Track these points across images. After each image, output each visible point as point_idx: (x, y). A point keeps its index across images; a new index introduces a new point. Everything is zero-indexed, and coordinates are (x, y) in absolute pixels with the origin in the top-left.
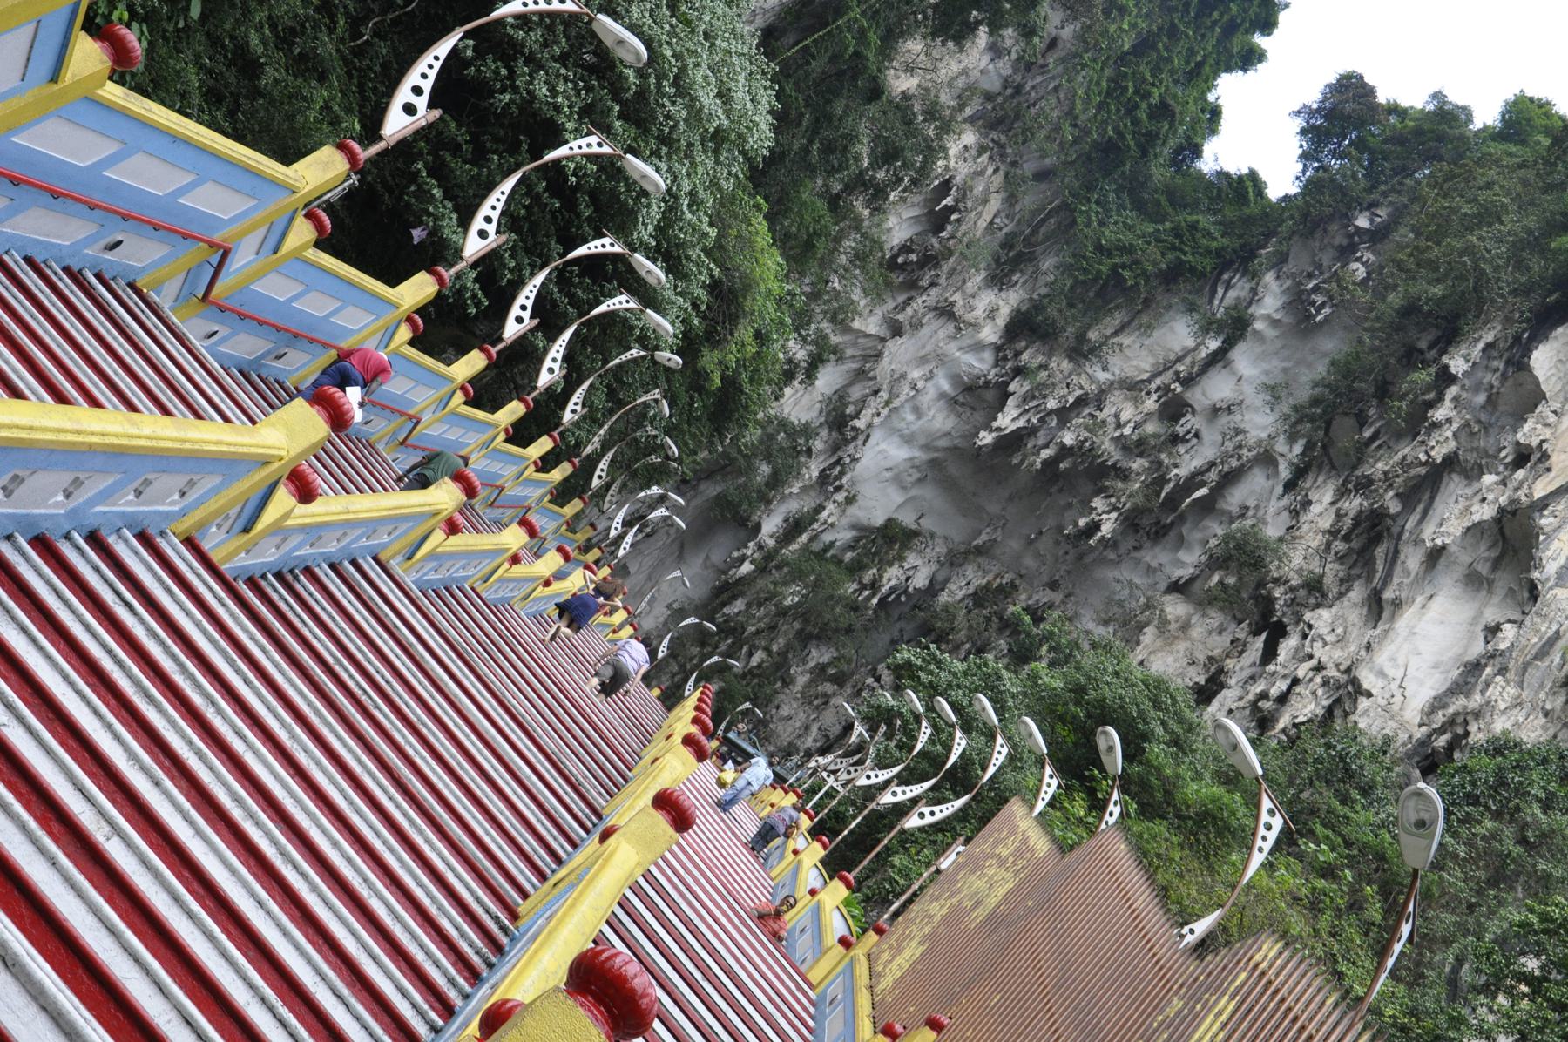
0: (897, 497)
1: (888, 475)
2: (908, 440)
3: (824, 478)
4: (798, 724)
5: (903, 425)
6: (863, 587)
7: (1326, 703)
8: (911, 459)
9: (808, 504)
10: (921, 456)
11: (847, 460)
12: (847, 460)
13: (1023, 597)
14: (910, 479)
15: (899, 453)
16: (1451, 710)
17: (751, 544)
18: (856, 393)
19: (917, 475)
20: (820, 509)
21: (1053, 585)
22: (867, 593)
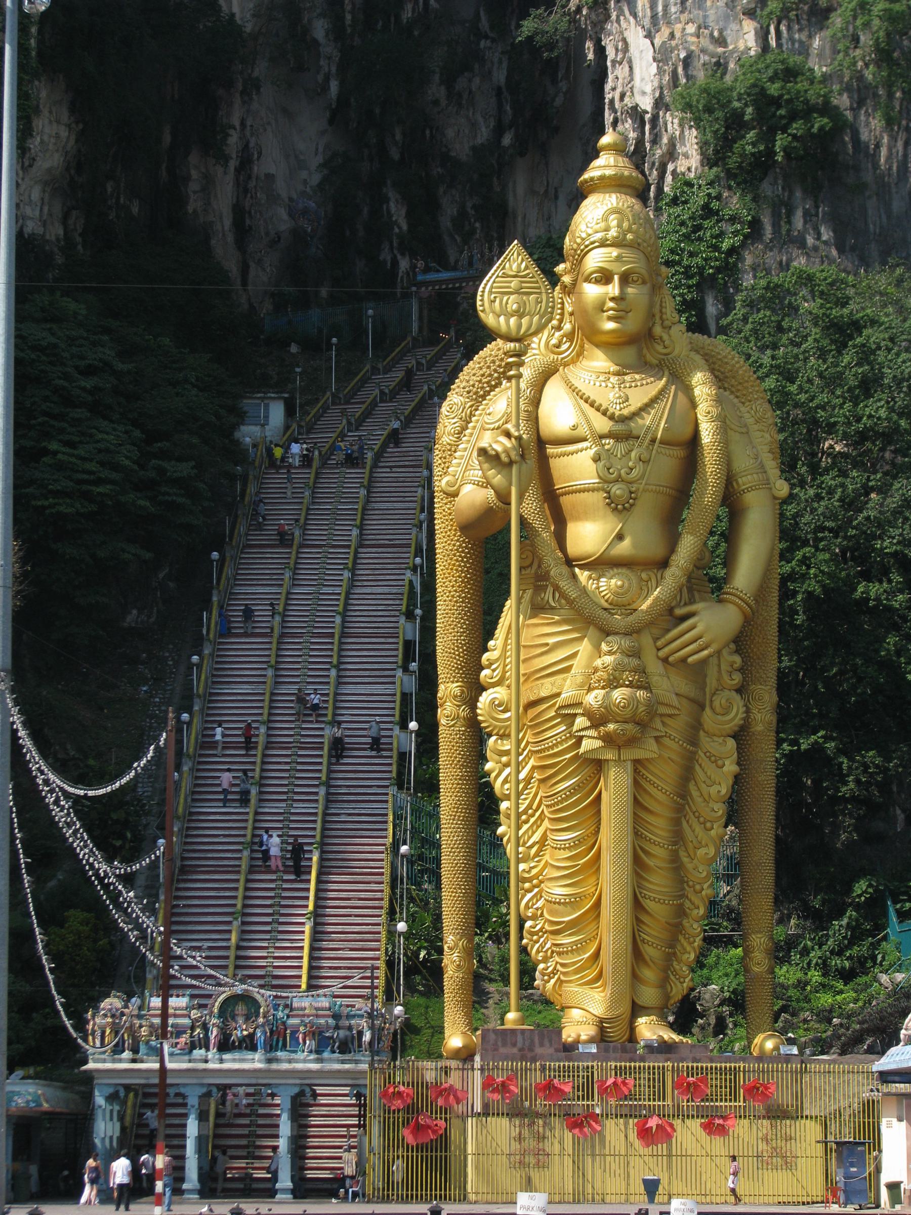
4: (467, 131)
17: (322, 63)
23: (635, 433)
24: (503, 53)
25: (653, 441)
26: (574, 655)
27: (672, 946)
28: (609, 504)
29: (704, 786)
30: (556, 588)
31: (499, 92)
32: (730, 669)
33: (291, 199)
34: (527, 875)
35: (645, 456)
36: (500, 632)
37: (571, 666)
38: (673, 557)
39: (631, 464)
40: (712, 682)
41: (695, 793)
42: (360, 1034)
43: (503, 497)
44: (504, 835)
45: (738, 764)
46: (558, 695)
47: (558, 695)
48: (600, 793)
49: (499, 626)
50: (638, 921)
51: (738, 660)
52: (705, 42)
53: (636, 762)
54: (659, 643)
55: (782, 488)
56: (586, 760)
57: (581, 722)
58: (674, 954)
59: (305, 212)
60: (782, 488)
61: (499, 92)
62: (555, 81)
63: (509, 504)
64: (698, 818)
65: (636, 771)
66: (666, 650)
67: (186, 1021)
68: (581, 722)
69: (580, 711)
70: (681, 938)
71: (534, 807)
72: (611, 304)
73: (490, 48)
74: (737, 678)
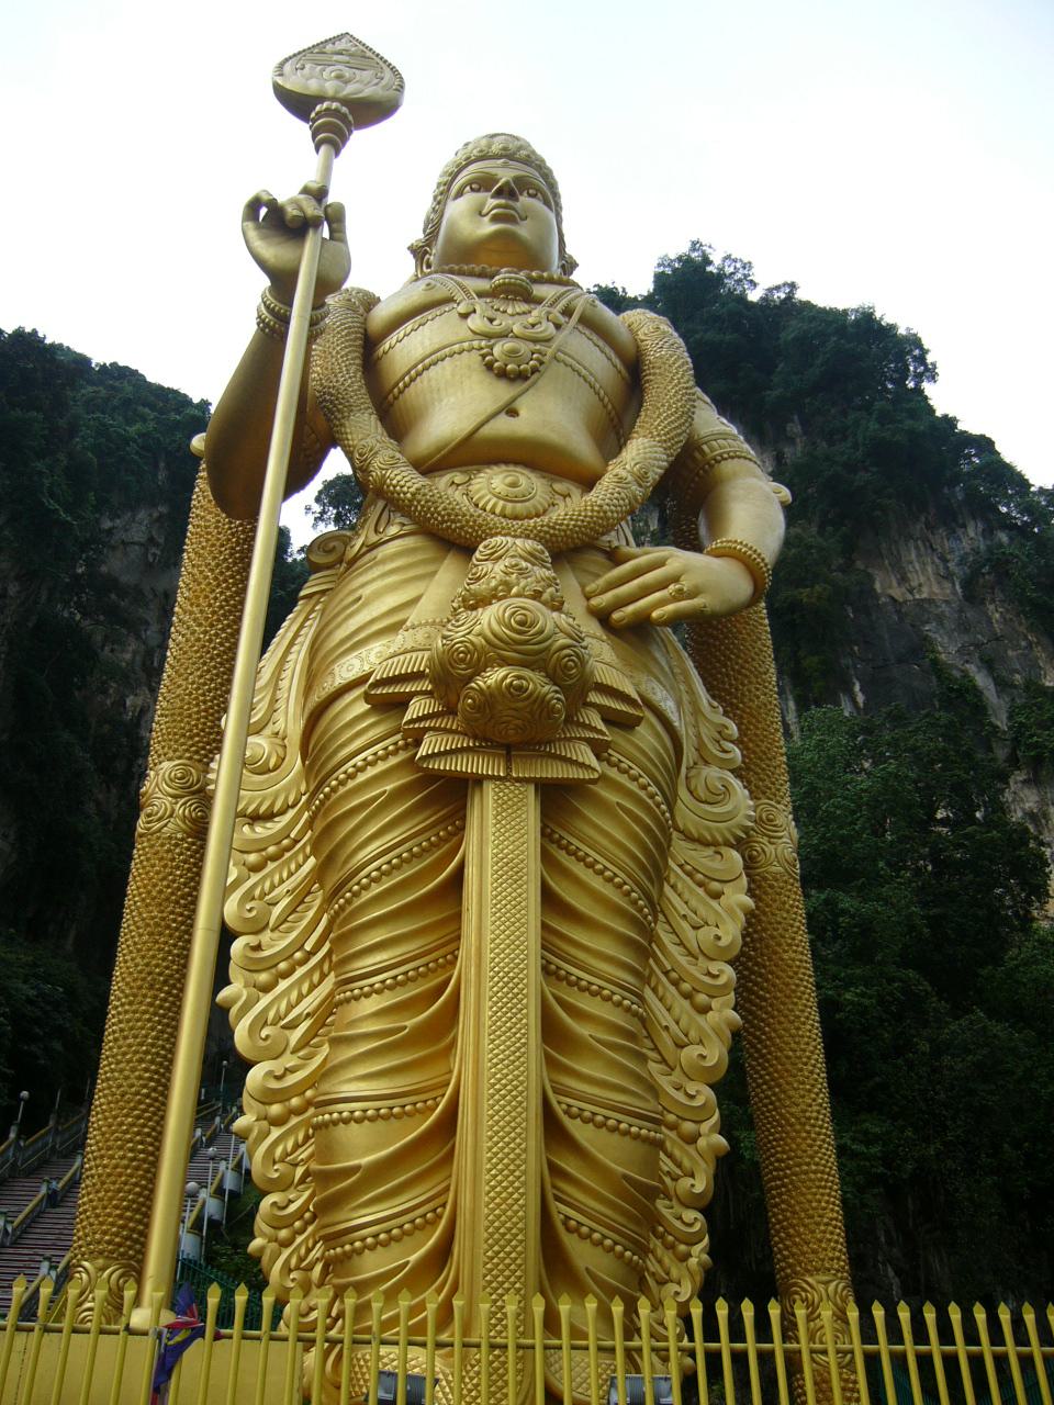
25: (568, 312)
26: (416, 600)
28: (489, 367)
29: (685, 925)
32: (718, 736)
34: (275, 1085)
37: (403, 622)
41: (667, 938)
44: (234, 1001)
45: (750, 892)
48: (461, 867)
64: (675, 983)
65: (543, 834)
66: (609, 596)
68: (417, 708)
69: (426, 686)
70: (655, 1243)
71: (308, 947)
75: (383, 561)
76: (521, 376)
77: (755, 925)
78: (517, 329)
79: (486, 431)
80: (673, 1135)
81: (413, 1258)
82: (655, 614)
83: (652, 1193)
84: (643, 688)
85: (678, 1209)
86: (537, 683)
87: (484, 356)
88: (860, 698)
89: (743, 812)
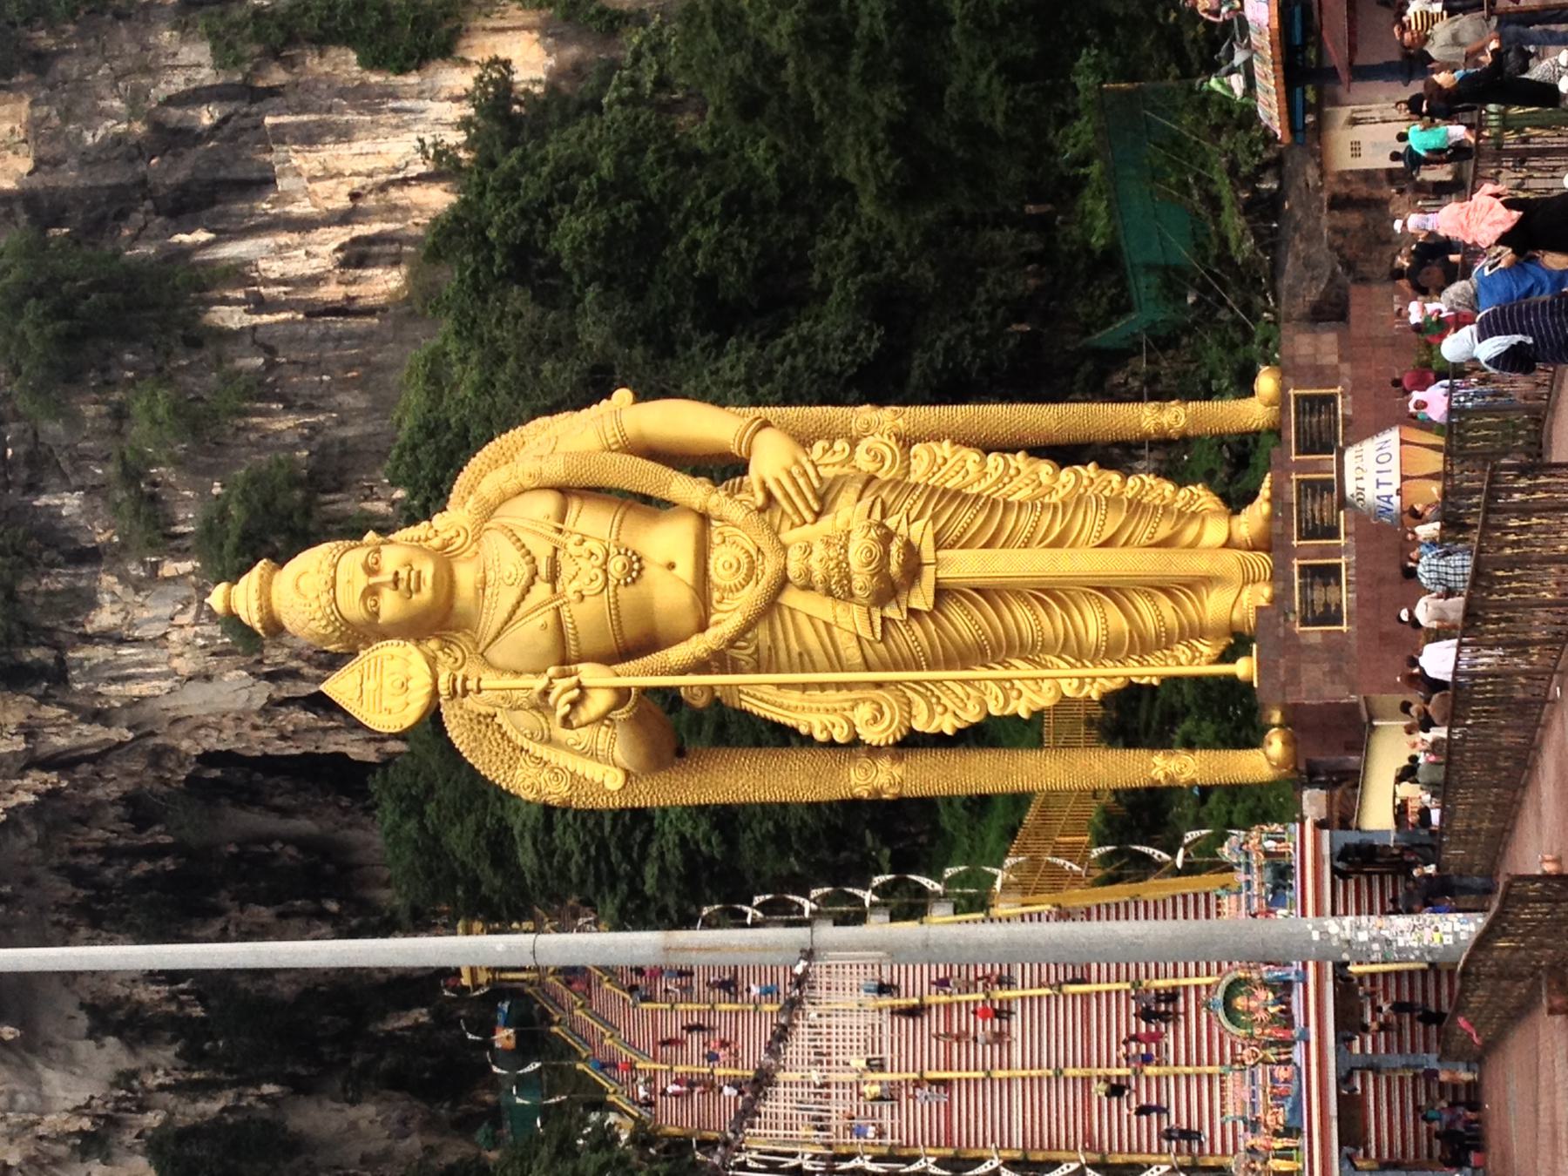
0: (85, 1048)
1: (78, 1071)
2: (38, 1083)
3: (142, 1109)
5: (34, 1098)
6: (181, 1005)
7: (283, 709)
8: (49, 1064)
9: (168, 1098)
10: (39, 1067)
11: (110, 1105)
12: (110, 1105)
13: (63, 894)
14: (61, 1052)
15: (53, 1079)
16: (318, 672)
17: (244, 1104)
18: (61, 1150)
19: (52, 1052)
20: (162, 1088)
21: (30, 882)
22: (183, 997)
23: (550, 552)
24: (242, 911)
25: (560, 531)
27: (1156, 508)
28: (634, 581)
30: (731, 643)
31: (281, 916)
33: (389, 1137)
35: (577, 538)
36: (788, 719)
38: (696, 506)
39: (586, 555)
40: (846, 470)
41: (975, 490)
42: (1267, 854)
43: (622, 694)
45: (938, 438)
46: (858, 637)
47: (858, 637)
49: (782, 720)
50: (1125, 544)
51: (819, 445)
52: (187, 618)
53: (938, 548)
54: (797, 521)
55: (623, 395)
56: (935, 606)
57: (892, 612)
58: (1165, 507)
59: (404, 1122)
60: (623, 395)
61: (281, 916)
62: (274, 855)
63: (629, 689)
67: (1259, 1070)
70: (1145, 500)
72: (402, 586)
73: (237, 925)
74: (840, 445)
75: (774, 639)
76: (639, 560)
77: (963, 440)
78: (599, 562)
79: (690, 582)
80: (1090, 490)
81: (1170, 603)
82: (816, 484)
83: (1130, 501)
84: (855, 497)
85: (1127, 489)
86: (894, 548)
87: (626, 584)
88: (202, 236)
89: (886, 439)
